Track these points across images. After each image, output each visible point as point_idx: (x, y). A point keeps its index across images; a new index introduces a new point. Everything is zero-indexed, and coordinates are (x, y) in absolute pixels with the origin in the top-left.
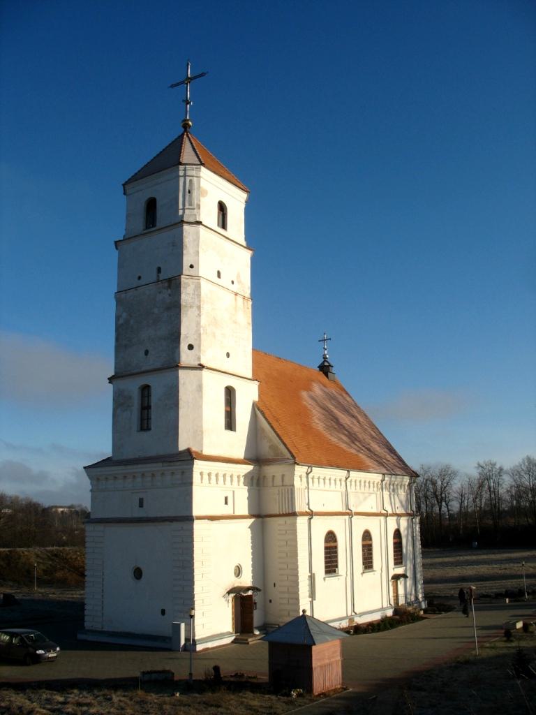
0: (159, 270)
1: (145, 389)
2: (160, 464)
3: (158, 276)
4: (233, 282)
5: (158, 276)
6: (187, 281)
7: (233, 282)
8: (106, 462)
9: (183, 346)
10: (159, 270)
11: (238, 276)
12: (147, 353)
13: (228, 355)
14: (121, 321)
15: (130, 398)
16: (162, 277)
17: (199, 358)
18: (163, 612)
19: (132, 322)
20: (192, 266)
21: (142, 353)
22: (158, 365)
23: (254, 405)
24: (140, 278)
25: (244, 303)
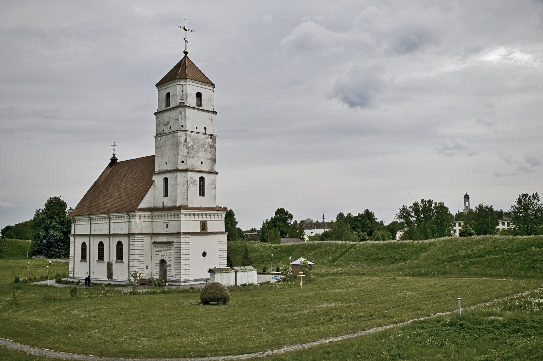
0: (205, 128)
1: (202, 179)
10: (205, 128)
12: (202, 163)
14: (189, 145)
15: (196, 181)
19: (195, 147)
22: (207, 170)
24: (197, 128)
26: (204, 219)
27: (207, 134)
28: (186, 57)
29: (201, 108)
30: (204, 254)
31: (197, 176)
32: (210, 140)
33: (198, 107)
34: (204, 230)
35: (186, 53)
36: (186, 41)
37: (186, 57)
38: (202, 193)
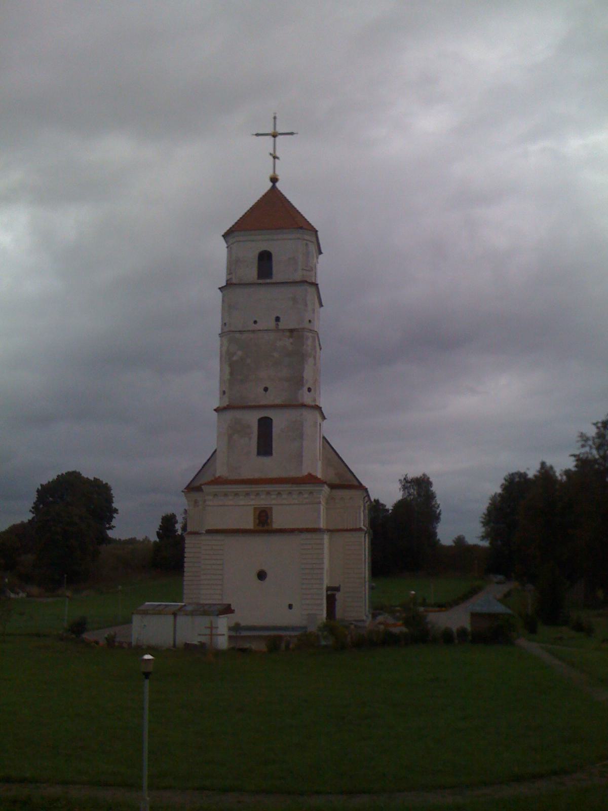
2: (290, 485)
5: (277, 325)
6: (308, 334)
9: (305, 389)
12: (266, 389)
14: (235, 358)
16: (282, 325)
17: (315, 400)
18: (290, 606)
21: (262, 390)
22: (278, 401)
26: (263, 502)
27: (283, 330)
28: (274, 188)
29: (268, 281)
30: (262, 575)
31: (252, 419)
32: (287, 342)
33: (260, 281)
34: (263, 522)
35: (274, 180)
36: (275, 157)
37: (274, 188)
38: (265, 447)
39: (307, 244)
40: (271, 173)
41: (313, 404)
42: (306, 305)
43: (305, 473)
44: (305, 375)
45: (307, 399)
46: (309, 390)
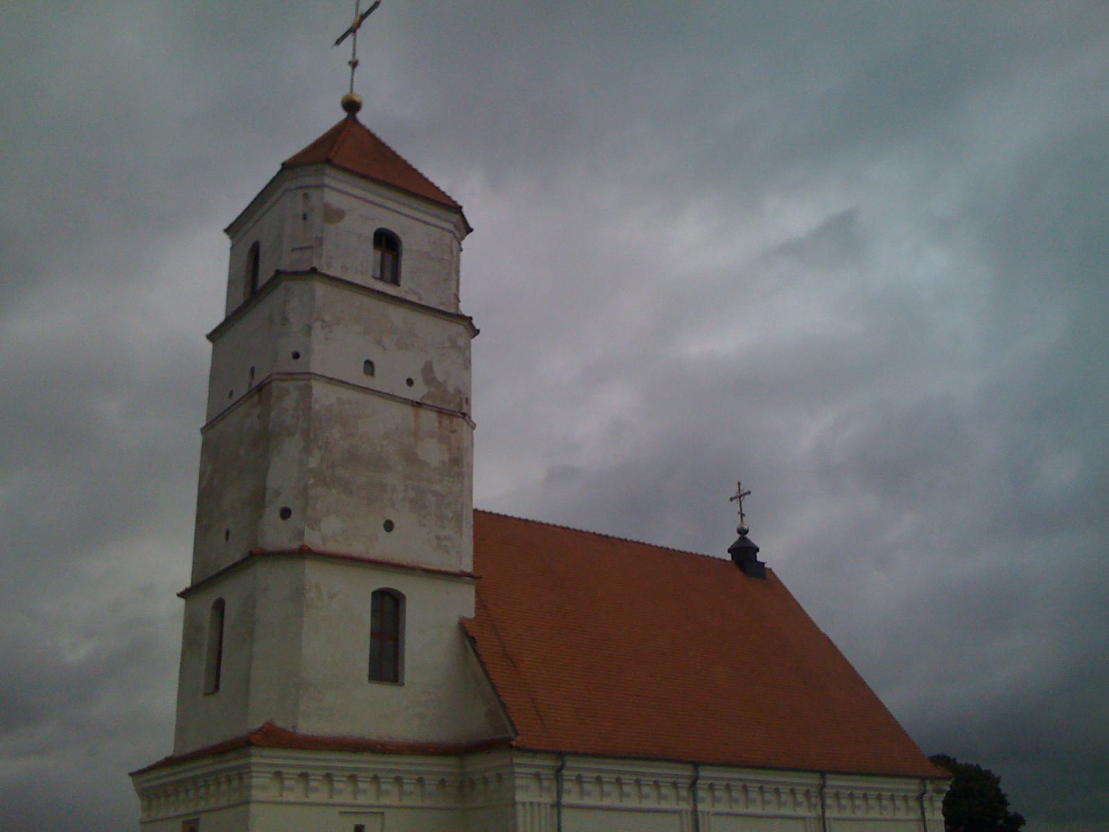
3: (250, 385)
4: (410, 382)
6: (284, 385)
7: (410, 382)
8: (168, 762)
11: (428, 370)
13: (389, 526)
17: (301, 534)
20: (296, 356)
23: (464, 628)
24: (231, 394)
25: (440, 422)
35: (351, 106)
36: (354, 64)
39: (306, 196)
40: (344, 92)
41: (295, 545)
42: (285, 320)
43: (256, 723)
44: (272, 483)
45: (276, 535)
46: (286, 513)
